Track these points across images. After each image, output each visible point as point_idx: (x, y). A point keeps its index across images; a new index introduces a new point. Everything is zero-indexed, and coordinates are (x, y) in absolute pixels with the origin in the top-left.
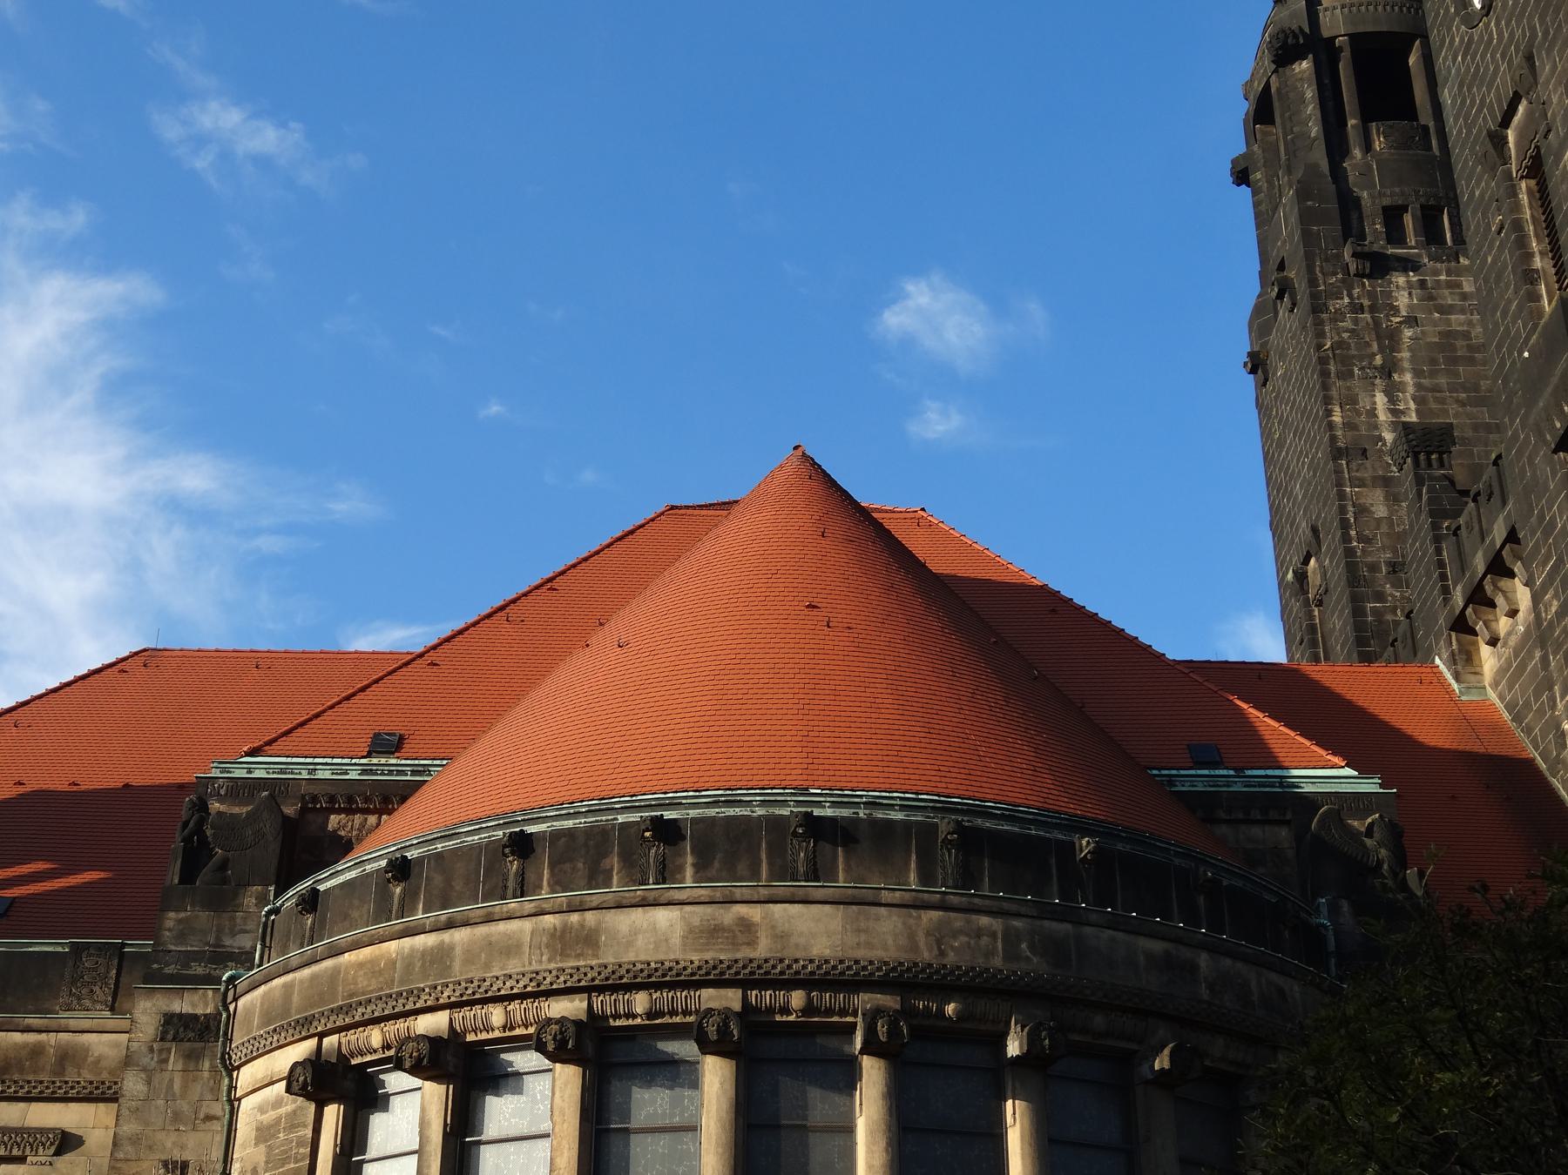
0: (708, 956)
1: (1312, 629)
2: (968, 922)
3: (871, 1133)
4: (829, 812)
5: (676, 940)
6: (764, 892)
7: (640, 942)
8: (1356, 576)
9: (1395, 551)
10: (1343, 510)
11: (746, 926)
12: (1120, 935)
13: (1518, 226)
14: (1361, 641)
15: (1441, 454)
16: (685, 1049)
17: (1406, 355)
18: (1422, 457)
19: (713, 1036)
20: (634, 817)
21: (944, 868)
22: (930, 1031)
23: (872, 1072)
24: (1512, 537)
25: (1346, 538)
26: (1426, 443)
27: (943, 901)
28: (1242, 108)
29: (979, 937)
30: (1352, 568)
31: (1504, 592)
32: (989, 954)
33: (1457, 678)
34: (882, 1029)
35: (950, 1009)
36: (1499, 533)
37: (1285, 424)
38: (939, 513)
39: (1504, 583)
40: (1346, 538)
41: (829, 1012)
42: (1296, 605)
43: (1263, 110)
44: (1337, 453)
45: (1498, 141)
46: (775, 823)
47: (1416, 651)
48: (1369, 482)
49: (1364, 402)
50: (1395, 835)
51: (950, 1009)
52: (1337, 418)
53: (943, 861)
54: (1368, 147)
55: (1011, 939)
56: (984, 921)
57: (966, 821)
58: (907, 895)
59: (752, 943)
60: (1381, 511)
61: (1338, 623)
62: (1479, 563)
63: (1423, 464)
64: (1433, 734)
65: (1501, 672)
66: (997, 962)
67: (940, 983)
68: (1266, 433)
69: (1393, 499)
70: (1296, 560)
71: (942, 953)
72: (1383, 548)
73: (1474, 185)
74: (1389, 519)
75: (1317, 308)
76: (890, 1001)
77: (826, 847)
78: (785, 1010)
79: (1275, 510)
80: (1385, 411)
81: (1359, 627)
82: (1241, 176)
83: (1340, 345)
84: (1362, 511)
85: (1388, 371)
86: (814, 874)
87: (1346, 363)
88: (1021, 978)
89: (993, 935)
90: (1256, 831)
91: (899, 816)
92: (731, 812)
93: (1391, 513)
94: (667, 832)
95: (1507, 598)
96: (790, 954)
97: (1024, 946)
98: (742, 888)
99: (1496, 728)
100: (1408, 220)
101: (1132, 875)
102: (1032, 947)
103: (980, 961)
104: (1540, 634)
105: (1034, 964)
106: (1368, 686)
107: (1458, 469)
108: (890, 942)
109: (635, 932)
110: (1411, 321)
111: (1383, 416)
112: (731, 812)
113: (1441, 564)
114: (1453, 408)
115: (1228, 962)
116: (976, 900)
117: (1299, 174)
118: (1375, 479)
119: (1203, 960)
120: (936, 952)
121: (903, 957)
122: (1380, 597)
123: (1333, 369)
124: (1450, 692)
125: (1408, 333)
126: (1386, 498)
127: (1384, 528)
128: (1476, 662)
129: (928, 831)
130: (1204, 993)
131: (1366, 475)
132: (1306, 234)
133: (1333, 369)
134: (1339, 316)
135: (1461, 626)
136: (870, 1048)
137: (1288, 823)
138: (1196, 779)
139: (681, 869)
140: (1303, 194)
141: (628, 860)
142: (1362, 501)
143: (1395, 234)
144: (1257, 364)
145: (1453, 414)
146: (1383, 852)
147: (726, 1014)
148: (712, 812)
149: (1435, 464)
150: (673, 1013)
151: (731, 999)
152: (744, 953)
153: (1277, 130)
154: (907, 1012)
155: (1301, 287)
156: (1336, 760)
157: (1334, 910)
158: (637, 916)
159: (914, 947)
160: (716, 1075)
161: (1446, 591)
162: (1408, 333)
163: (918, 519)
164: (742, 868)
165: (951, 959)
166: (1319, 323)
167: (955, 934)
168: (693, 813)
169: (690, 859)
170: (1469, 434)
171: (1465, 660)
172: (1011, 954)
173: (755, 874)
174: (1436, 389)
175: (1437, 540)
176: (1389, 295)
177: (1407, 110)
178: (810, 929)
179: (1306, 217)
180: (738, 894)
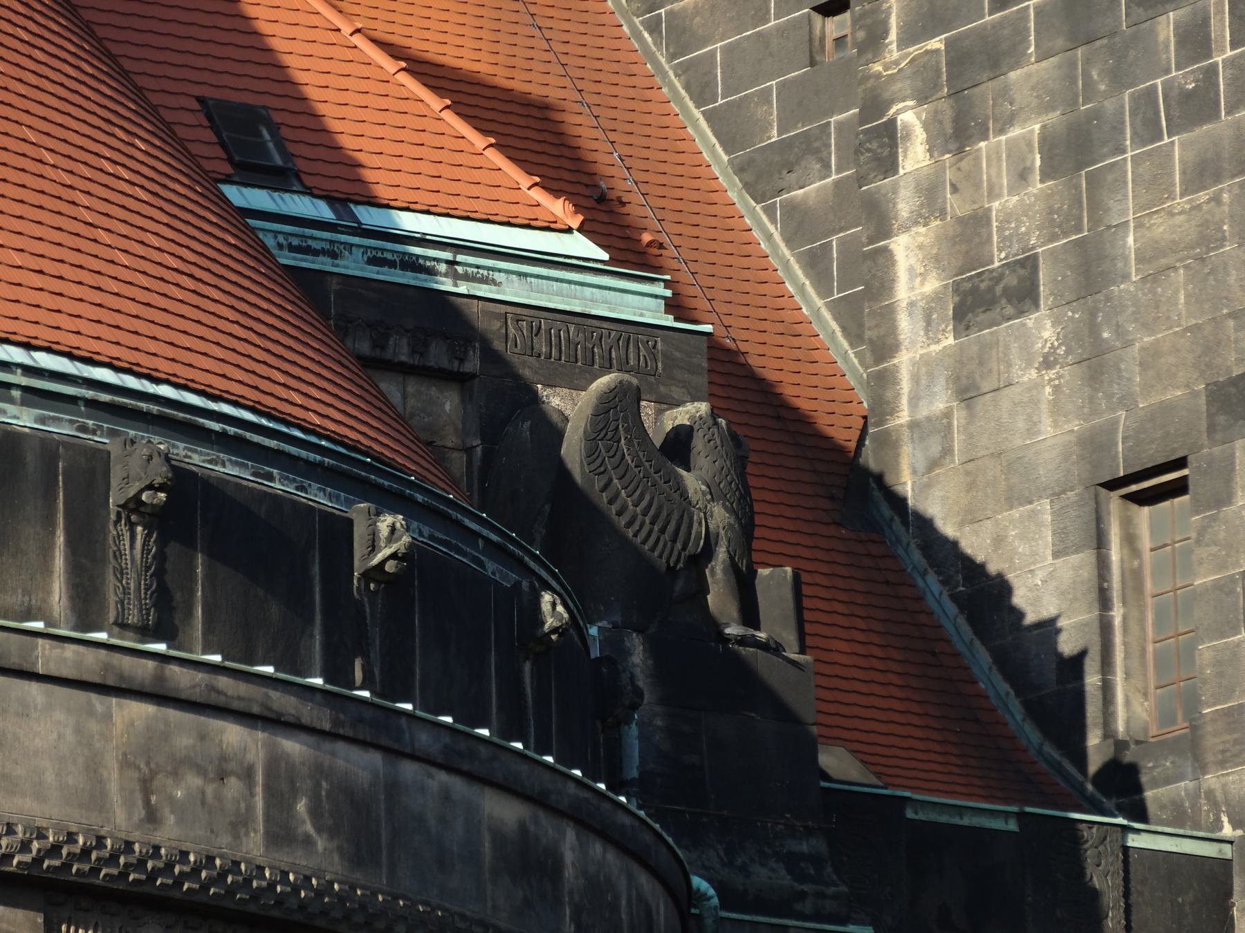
2: (202, 737)
12: (457, 785)
21: (120, 573)
27: (160, 678)
53: (118, 555)
56: (233, 734)
57: (197, 458)
58: (92, 658)
66: (254, 846)
71: (152, 817)
88: (296, 889)
89: (247, 775)
97: (301, 806)
102: (315, 812)
108: (50, 777)
116: (223, 682)
120: (140, 812)
121: (76, 818)
129: (91, 471)
137: (460, 379)
146: (720, 517)
156: (558, 208)
159: (97, 799)
165: (169, 834)
167: (178, 766)
172: (281, 833)
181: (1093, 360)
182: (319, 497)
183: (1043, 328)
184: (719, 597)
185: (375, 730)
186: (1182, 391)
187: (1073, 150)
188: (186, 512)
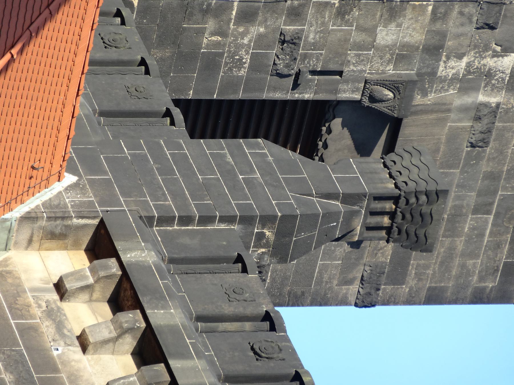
9: (315, 46)
15: (389, 230)
18: (389, 206)
31: (115, 340)
33: (28, 218)
39: (129, 343)
47: (82, 160)
48: (438, 26)
60: (386, 36)
62: (167, 316)
63: (378, 206)
69: (402, 55)
72: (326, 32)
74: (372, 45)
93: (381, 50)
95: (106, 342)
113: (206, 220)
118: (443, 35)
126: (405, 46)
127: (356, 37)
128: (47, 244)
131: (453, 25)
142: (409, 13)
149: (374, 220)
170: (485, 167)
171: (52, 229)
175: (247, 220)
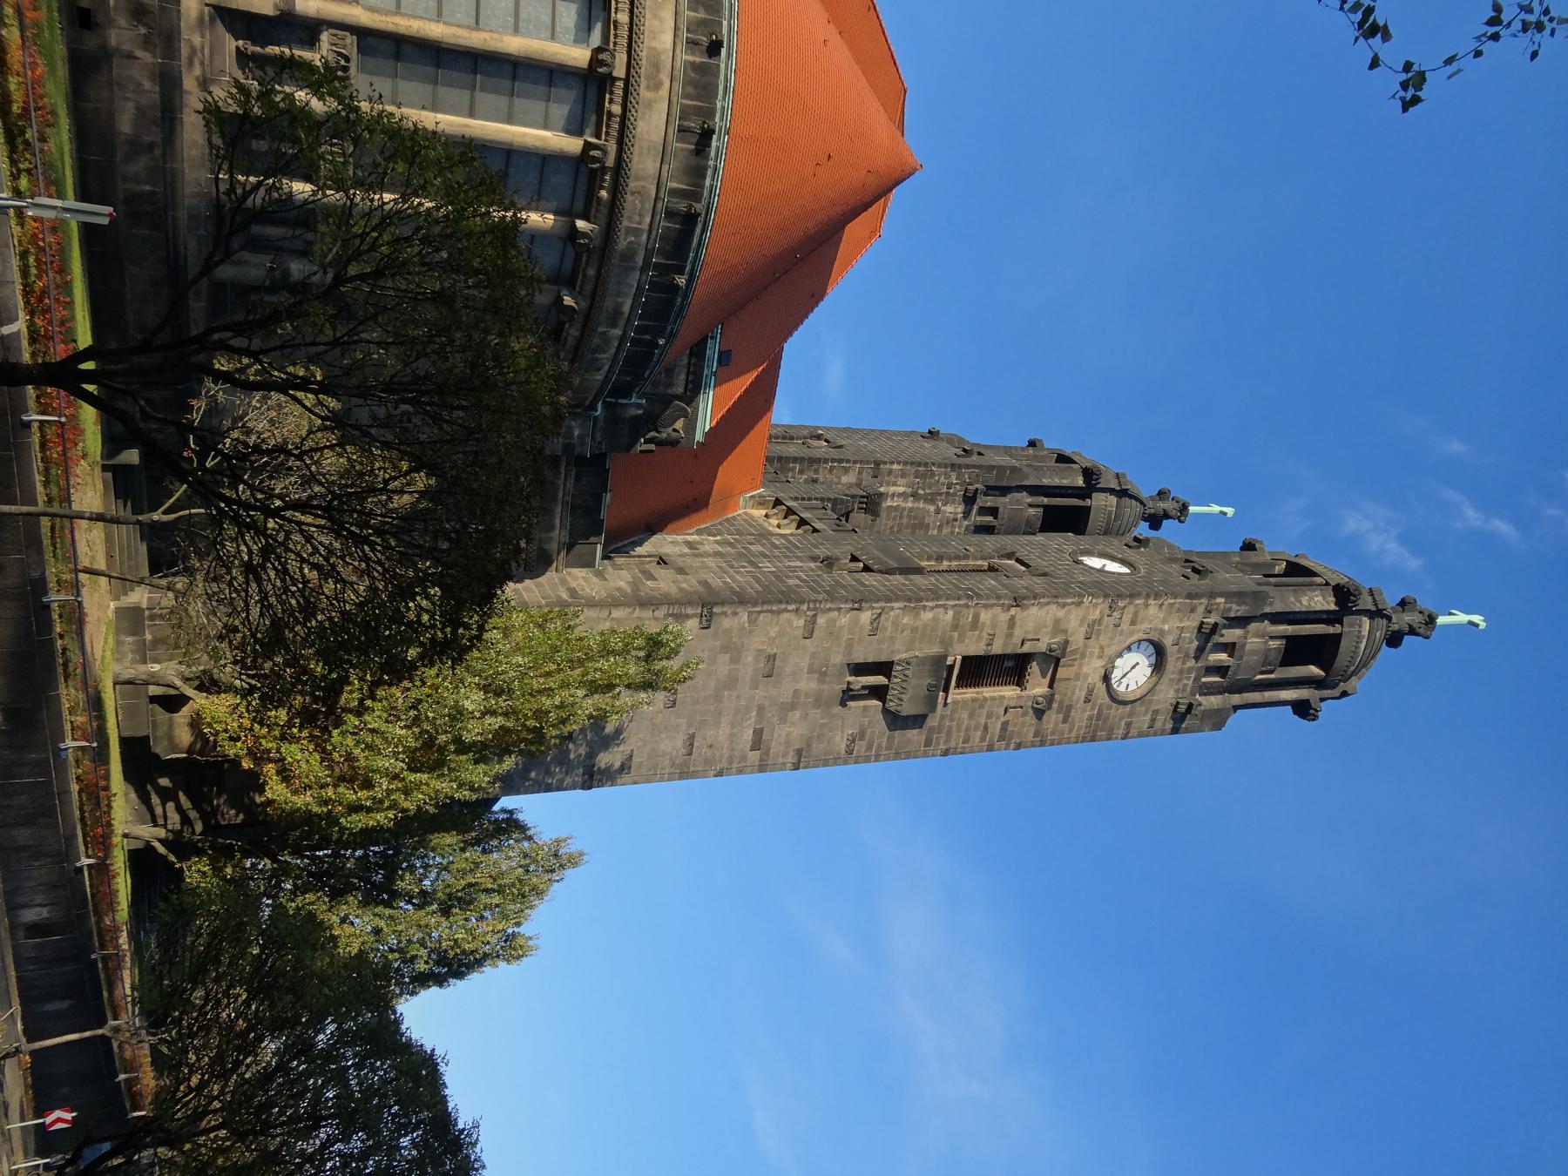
0: (644, 62)
1: (792, 438)
3: (543, 139)
4: (714, 144)
5: (654, 44)
6: (674, 99)
7: (656, 23)
8: (813, 461)
10: (848, 461)
11: (657, 86)
13: (966, 557)
14: (780, 459)
16: (596, 39)
17: (921, 505)
19: (601, 57)
20: (725, 31)
22: (594, 179)
23: (573, 145)
24: (815, 530)
25: (833, 460)
26: (871, 504)
28: (1068, 451)
29: (640, 216)
30: (818, 461)
32: (630, 219)
34: (594, 153)
35: (604, 193)
36: (818, 525)
37: (899, 442)
38: (876, 245)
39: (794, 525)
40: (833, 460)
41: (608, 126)
42: (805, 433)
43: (1063, 459)
44: (877, 464)
45: (1010, 556)
46: (711, 113)
49: (900, 481)
50: (673, 443)
51: (604, 193)
52: (895, 466)
54: (1031, 506)
55: (636, 232)
56: (648, 219)
59: (648, 88)
60: (844, 479)
61: (792, 450)
62: (805, 515)
64: (726, 474)
65: (752, 517)
66: (625, 223)
67: (617, 190)
68: (896, 433)
69: (850, 486)
70: (828, 437)
71: (633, 193)
73: (990, 542)
75: (953, 466)
76: (610, 161)
77: (695, 140)
78: (611, 101)
79: (856, 431)
80: (895, 492)
81: (788, 459)
82: (1032, 444)
83: (933, 474)
84: (846, 470)
85: (915, 495)
86: (682, 130)
87: (924, 476)
90: (683, 377)
91: (708, 182)
92: (721, 88)
94: (714, 48)
96: (640, 108)
98: (678, 87)
99: (724, 509)
100: (990, 518)
101: (664, 303)
103: (626, 213)
104: (764, 535)
105: (622, 243)
106: (752, 449)
107: (858, 518)
109: (661, 20)
110: (938, 511)
111: (892, 489)
112: (721, 88)
114: (890, 523)
115: (616, 344)
117: (1025, 469)
119: (618, 332)
121: (632, 173)
122: (801, 472)
123: (922, 468)
124: (746, 491)
125: (932, 508)
129: (697, 197)
130: (601, 329)
132: (992, 467)
133: (922, 468)
134: (947, 476)
135: (778, 502)
136: (587, 144)
138: (713, 350)
139: (693, 54)
140: (1014, 470)
141: (702, 23)
143: (984, 511)
144: (933, 434)
145: (884, 522)
146: (664, 435)
147: (611, 66)
148: (722, 77)
150: (616, 36)
151: (619, 72)
152: (643, 82)
153: (1053, 464)
154: (604, 169)
155: (967, 461)
157: (639, 406)
158: (670, 23)
159: (637, 179)
160: (578, 56)
161: (796, 499)
162: (932, 508)
163: (874, 232)
164: (690, 90)
165: (629, 197)
166: (946, 466)
167: (642, 202)
168: (723, 66)
169: (698, 60)
171: (760, 502)
172: (629, 231)
173: (685, 96)
174: (901, 517)
175: (822, 499)
176: (953, 502)
177: (1045, 528)
178: (653, 122)
179: (1001, 469)
180: (675, 84)
181: (681, 556)
182: (688, 268)
183: (686, 550)
184: (652, 434)
185: (649, 253)
186: (680, 564)
187: (717, 554)
188: (690, 219)
